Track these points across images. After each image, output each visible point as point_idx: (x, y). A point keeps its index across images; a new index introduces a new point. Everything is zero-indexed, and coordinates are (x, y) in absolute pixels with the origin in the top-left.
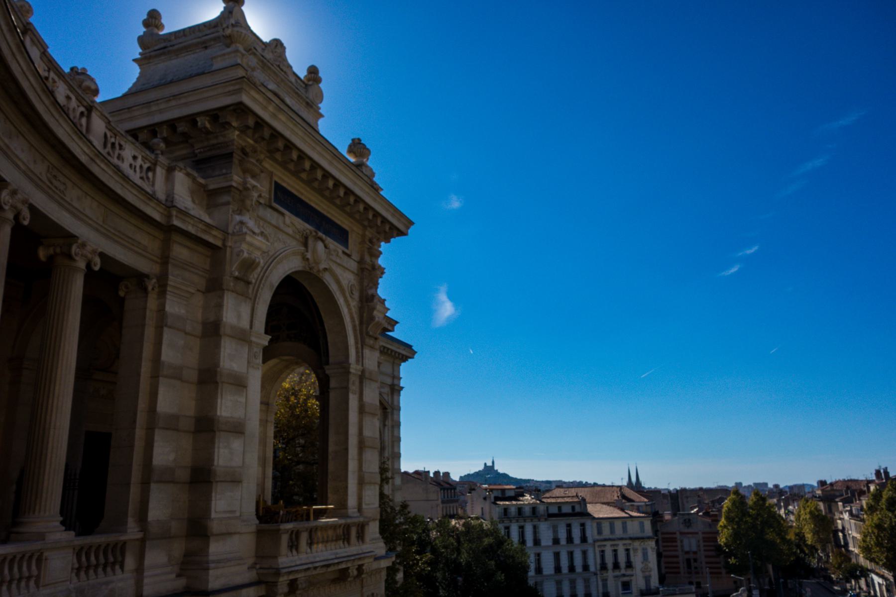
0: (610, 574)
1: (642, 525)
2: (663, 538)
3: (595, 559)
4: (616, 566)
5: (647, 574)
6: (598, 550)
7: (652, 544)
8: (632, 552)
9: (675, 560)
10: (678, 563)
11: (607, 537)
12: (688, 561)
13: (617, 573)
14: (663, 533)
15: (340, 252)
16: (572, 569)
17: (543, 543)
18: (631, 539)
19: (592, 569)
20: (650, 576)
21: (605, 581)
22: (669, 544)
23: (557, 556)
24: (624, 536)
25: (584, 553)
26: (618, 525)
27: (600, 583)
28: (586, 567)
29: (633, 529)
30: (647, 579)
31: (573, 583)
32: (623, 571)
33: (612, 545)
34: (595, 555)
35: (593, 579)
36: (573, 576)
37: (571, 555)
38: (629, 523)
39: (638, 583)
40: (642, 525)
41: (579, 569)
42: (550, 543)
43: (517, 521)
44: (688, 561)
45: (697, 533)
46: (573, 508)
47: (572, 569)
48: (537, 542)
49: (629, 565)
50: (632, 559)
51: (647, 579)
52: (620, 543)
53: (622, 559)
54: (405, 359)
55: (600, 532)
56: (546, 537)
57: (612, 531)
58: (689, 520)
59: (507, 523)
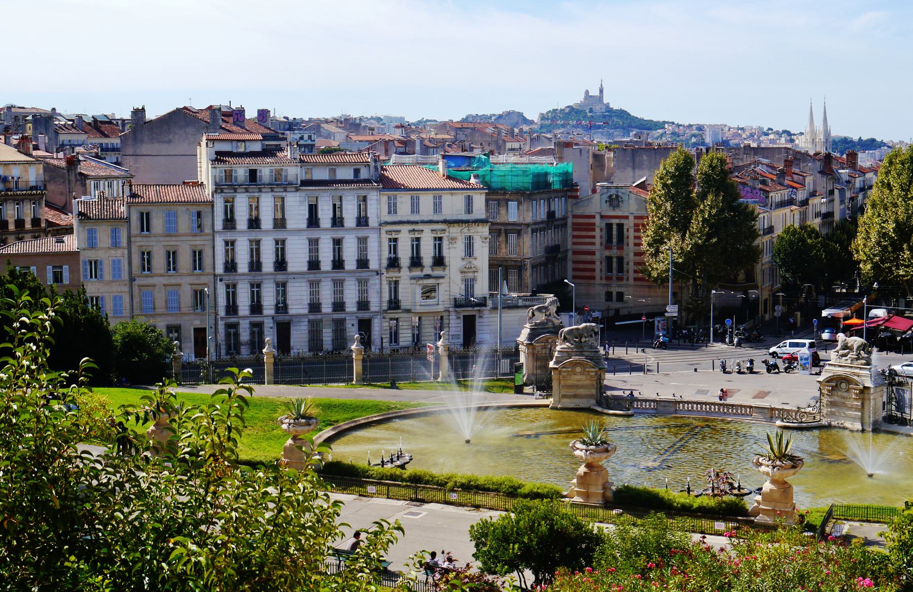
0: (404, 275)
1: (469, 200)
2: (574, 224)
3: (380, 251)
4: (416, 262)
5: (470, 275)
6: (385, 238)
7: (485, 230)
8: (445, 243)
9: (589, 258)
10: (593, 263)
11: (405, 219)
12: (609, 259)
13: (417, 273)
14: (575, 216)
16: (338, 264)
17: (290, 225)
18: (445, 222)
19: (373, 265)
20: (473, 280)
22: (585, 233)
23: (314, 244)
24: (436, 218)
25: (363, 241)
26: (426, 202)
27: (386, 288)
28: (363, 263)
29: (453, 206)
30: (469, 285)
31: (338, 285)
32: (427, 271)
33: (410, 231)
34: (380, 242)
35: (374, 281)
36: (339, 275)
37: (338, 242)
38: (446, 199)
39: (451, 286)
40: (469, 200)
41: (350, 263)
42: (304, 224)
44: (609, 259)
45: (627, 217)
46: (357, 172)
47: (338, 264)
48: (280, 223)
49: (439, 261)
50: (445, 253)
51: (469, 285)
52: (427, 228)
53: (427, 254)
56: (297, 214)
58: (617, 196)
59: (229, 194)
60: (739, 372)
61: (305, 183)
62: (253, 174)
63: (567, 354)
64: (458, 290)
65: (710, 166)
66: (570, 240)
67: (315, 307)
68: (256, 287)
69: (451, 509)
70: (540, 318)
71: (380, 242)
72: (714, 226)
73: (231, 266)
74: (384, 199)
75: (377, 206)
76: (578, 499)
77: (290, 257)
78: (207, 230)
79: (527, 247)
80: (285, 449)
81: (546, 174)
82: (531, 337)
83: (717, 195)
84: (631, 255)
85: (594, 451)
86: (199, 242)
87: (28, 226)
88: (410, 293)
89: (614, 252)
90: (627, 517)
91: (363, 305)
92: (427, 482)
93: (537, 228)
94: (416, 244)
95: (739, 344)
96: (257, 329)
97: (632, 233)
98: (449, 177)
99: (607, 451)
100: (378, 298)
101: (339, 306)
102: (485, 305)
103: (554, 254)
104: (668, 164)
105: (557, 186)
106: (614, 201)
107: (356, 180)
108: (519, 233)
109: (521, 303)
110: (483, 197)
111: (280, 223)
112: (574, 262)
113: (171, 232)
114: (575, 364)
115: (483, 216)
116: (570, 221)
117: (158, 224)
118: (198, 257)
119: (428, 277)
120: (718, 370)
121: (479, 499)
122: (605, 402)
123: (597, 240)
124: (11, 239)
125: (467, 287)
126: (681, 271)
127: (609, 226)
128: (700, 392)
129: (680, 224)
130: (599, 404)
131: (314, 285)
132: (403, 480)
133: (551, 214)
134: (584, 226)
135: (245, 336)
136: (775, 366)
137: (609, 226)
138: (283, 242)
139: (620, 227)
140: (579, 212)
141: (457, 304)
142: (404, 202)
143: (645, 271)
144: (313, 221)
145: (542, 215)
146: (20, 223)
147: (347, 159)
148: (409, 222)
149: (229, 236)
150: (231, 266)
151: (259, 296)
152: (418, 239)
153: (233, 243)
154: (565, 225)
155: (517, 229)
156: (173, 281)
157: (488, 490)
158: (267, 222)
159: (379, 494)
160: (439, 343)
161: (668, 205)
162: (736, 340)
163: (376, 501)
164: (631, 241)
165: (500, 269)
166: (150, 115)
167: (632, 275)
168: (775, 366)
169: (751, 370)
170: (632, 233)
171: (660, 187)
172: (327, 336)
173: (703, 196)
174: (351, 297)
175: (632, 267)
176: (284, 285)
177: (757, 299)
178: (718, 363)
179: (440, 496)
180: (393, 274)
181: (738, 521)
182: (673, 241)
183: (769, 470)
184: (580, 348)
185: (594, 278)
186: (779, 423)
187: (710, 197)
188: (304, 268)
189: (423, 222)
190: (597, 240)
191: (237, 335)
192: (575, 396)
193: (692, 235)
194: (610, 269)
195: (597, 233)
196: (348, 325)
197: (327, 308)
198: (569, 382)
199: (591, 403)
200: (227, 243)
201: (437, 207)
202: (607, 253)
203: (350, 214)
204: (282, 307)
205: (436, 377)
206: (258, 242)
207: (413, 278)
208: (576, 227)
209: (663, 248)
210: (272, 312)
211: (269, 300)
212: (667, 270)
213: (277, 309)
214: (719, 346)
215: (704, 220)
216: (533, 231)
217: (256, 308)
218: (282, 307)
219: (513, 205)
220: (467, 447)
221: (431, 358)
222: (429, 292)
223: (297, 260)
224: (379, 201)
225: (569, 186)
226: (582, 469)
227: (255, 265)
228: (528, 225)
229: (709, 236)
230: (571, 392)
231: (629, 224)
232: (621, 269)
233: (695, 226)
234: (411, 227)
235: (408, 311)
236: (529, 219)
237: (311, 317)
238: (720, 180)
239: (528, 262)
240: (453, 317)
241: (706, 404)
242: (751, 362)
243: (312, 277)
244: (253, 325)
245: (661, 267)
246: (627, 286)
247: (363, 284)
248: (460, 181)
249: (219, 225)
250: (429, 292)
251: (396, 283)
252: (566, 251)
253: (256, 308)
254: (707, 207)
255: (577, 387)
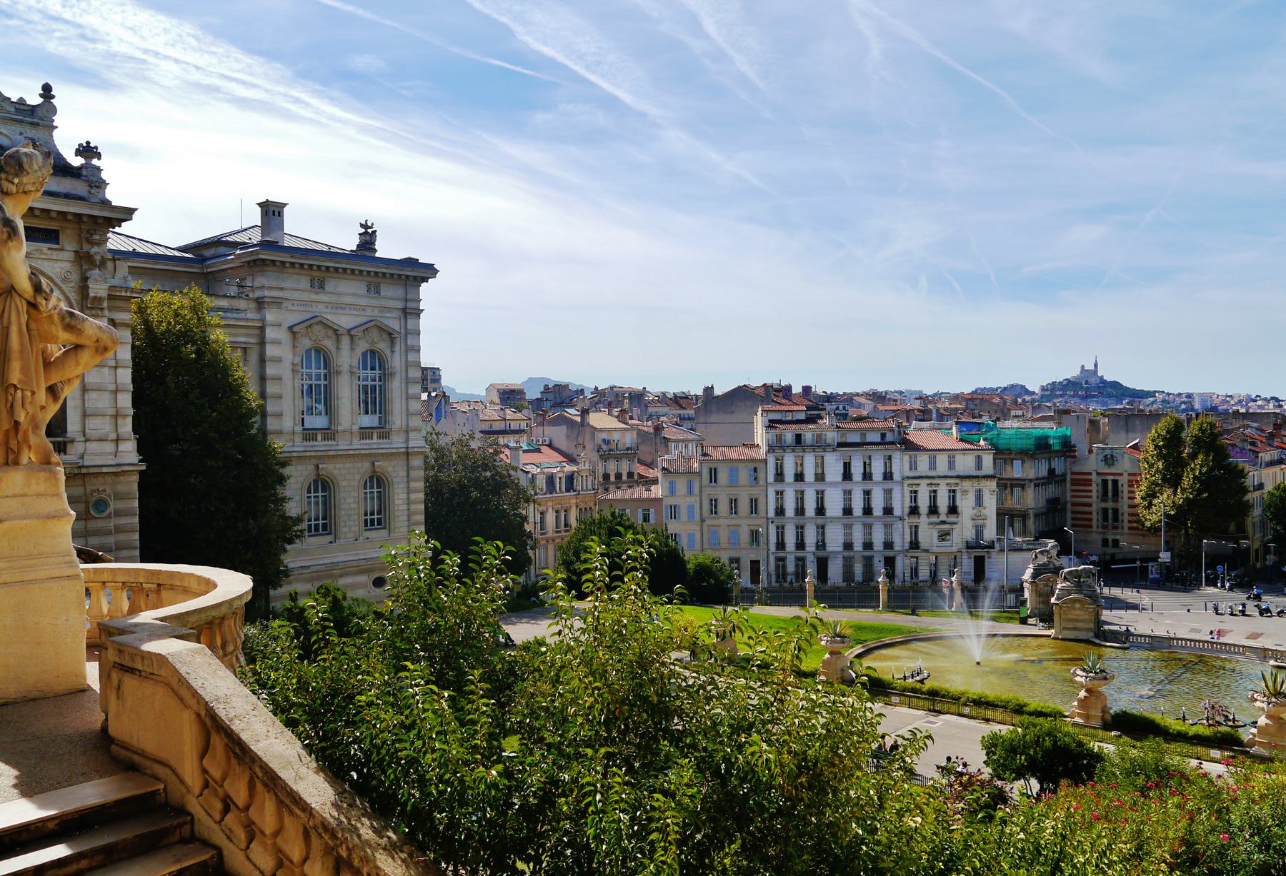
0: (923, 521)
1: (979, 459)
3: (903, 501)
4: (933, 510)
5: (980, 522)
6: (907, 490)
7: (993, 484)
9: (1086, 509)
12: (1105, 511)
13: (934, 519)
14: (1073, 473)
15: (45, 250)
16: (868, 511)
17: (828, 478)
18: (958, 477)
19: (897, 512)
20: (983, 526)
21: (915, 530)
23: (848, 494)
24: (950, 474)
25: (888, 493)
26: (942, 461)
28: (888, 511)
29: (965, 463)
30: (979, 530)
31: (868, 528)
32: (943, 518)
34: (903, 496)
35: (898, 526)
36: (868, 520)
37: (867, 493)
38: (959, 458)
39: (964, 530)
40: (979, 459)
41: (878, 509)
42: (840, 479)
43: (793, 451)
44: (1105, 511)
45: (1121, 474)
46: (883, 436)
47: (868, 511)
48: (820, 477)
49: (953, 510)
50: (958, 503)
51: (979, 530)
52: (943, 482)
54: (425, 280)
55: (913, 466)
57: (932, 465)
59: (779, 453)
60: (1232, 614)
61: (840, 445)
62: (798, 438)
63: (1066, 591)
64: (969, 534)
65: (1200, 429)
66: (1069, 494)
67: (848, 546)
68: (800, 529)
69: (964, 720)
70: (1043, 560)
71: (903, 496)
72: (1204, 482)
73: (780, 511)
74: (907, 458)
75: (900, 464)
76: (1077, 720)
77: (827, 505)
78: (762, 482)
79: (1030, 499)
80: (824, 662)
81: (1047, 437)
82: (1035, 576)
83: (1207, 455)
84: (1126, 507)
85: (1094, 678)
86: (755, 492)
87: (625, 478)
88: (928, 536)
89: (1110, 505)
90: (1125, 739)
91: (888, 545)
92: (943, 696)
93: (1039, 483)
94: (934, 495)
95: (1231, 589)
96: (801, 562)
97: (1126, 489)
98: (961, 440)
99: (1105, 678)
100: (901, 539)
101: (868, 545)
102: (993, 547)
103: (1054, 506)
104: (1160, 428)
105: (1057, 448)
106: (1109, 460)
107: (883, 442)
108: (1023, 487)
109: (1025, 546)
110: (991, 457)
111: (820, 477)
112: (1073, 512)
113: (733, 483)
114: (1075, 601)
115: (991, 472)
116: (1069, 477)
117: (723, 477)
118: (754, 504)
119: (944, 522)
120: (1211, 611)
121: (989, 713)
122: (1102, 635)
123: (1094, 494)
124: (612, 488)
125: (977, 532)
126: (1174, 522)
127: (1105, 482)
128: (1193, 630)
129: (1172, 480)
130: (1097, 636)
131: (848, 527)
132: (922, 693)
133: (1051, 471)
134: (1082, 481)
135: (791, 567)
136: (1268, 610)
137: (1105, 482)
138: (823, 492)
139: (1115, 482)
140: (1077, 469)
141: (969, 546)
142: (923, 460)
143: (1139, 521)
144: (847, 475)
145: (1043, 472)
146: (619, 476)
147: (875, 425)
148: (927, 477)
149: (779, 487)
150: (780, 511)
151: (802, 536)
152: (935, 491)
153: (782, 493)
154: (1064, 481)
155: (1021, 484)
156: (733, 522)
157: (997, 706)
158: (809, 476)
159: (902, 704)
160: (953, 579)
161: (1160, 464)
162: (1227, 585)
163: (898, 709)
164: (1126, 495)
165: (1006, 517)
166: (718, 392)
167: (1126, 525)
168: (1268, 610)
169: (1243, 613)
170: (1126, 489)
171: (1152, 447)
172: (858, 569)
173: (1193, 456)
174: (878, 539)
175: (1126, 518)
176: (823, 527)
177: (1248, 549)
178: (1210, 605)
179: (954, 708)
180: (914, 520)
181: (1233, 751)
182: (1165, 496)
183: (1265, 705)
184: (1079, 587)
185: (1091, 526)
186: (1272, 662)
187: (1200, 457)
188: (840, 513)
189: (939, 477)
190: (1094, 494)
191: (784, 567)
192: (1075, 629)
193: (1183, 490)
194: (1105, 518)
195: (1094, 488)
196: (876, 560)
197: (858, 546)
198: (1070, 616)
199: (1089, 636)
200: (777, 493)
201: (952, 464)
202: (1104, 505)
203: (877, 469)
204: (821, 545)
205: (951, 607)
206: (802, 492)
207: (931, 524)
208: (1074, 482)
209: (1155, 501)
210: (813, 549)
211: (810, 539)
212: (1160, 521)
213: (818, 547)
214: (1211, 590)
215: (1195, 477)
216: (1036, 485)
217: (800, 545)
218: (821, 545)
219: (1017, 463)
220: (977, 668)
221: (946, 591)
222: (944, 536)
223: (834, 505)
224: (902, 460)
225: (1067, 447)
226: (1082, 694)
227: (800, 511)
228: (1031, 480)
229: (1200, 492)
230: (1071, 625)
231: (1123, 480)
232: (1116, 519)
233: (1186, 482)
234: (929, 481)
235: (927, 551)
236: (1031, 475)
237: (846, 554)
238: (1210, 442)
239: (1031, 513)
240: (965, 556)
241: (1199, 641)
242: (1244, 605)
243: (845, 521)
244: (798, 559)
245: (1155, 518)
246: (1121, 534)
247: (888, 527)
248: (971, 443)
249: (771, 478)
250: (944, 536)
251: (916, 527)
252: (1066, 503)
253: (800, 545)
254: (1198, 466)
255: (1076, 620)
